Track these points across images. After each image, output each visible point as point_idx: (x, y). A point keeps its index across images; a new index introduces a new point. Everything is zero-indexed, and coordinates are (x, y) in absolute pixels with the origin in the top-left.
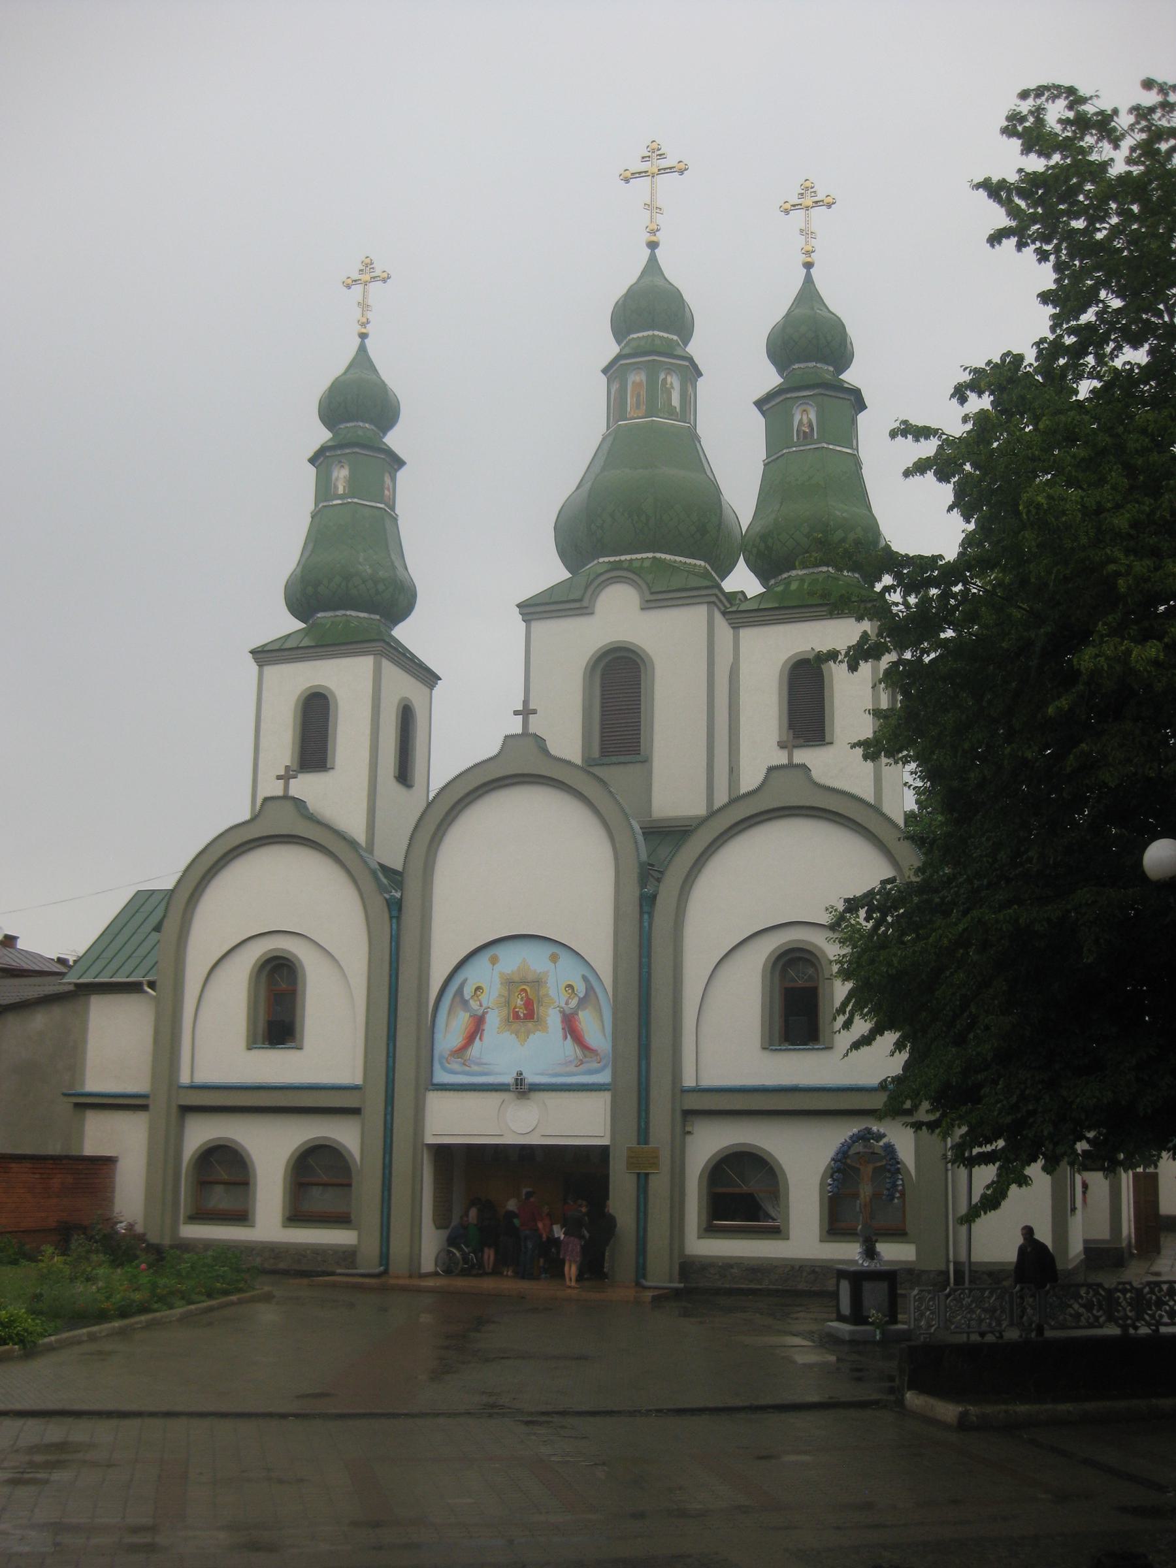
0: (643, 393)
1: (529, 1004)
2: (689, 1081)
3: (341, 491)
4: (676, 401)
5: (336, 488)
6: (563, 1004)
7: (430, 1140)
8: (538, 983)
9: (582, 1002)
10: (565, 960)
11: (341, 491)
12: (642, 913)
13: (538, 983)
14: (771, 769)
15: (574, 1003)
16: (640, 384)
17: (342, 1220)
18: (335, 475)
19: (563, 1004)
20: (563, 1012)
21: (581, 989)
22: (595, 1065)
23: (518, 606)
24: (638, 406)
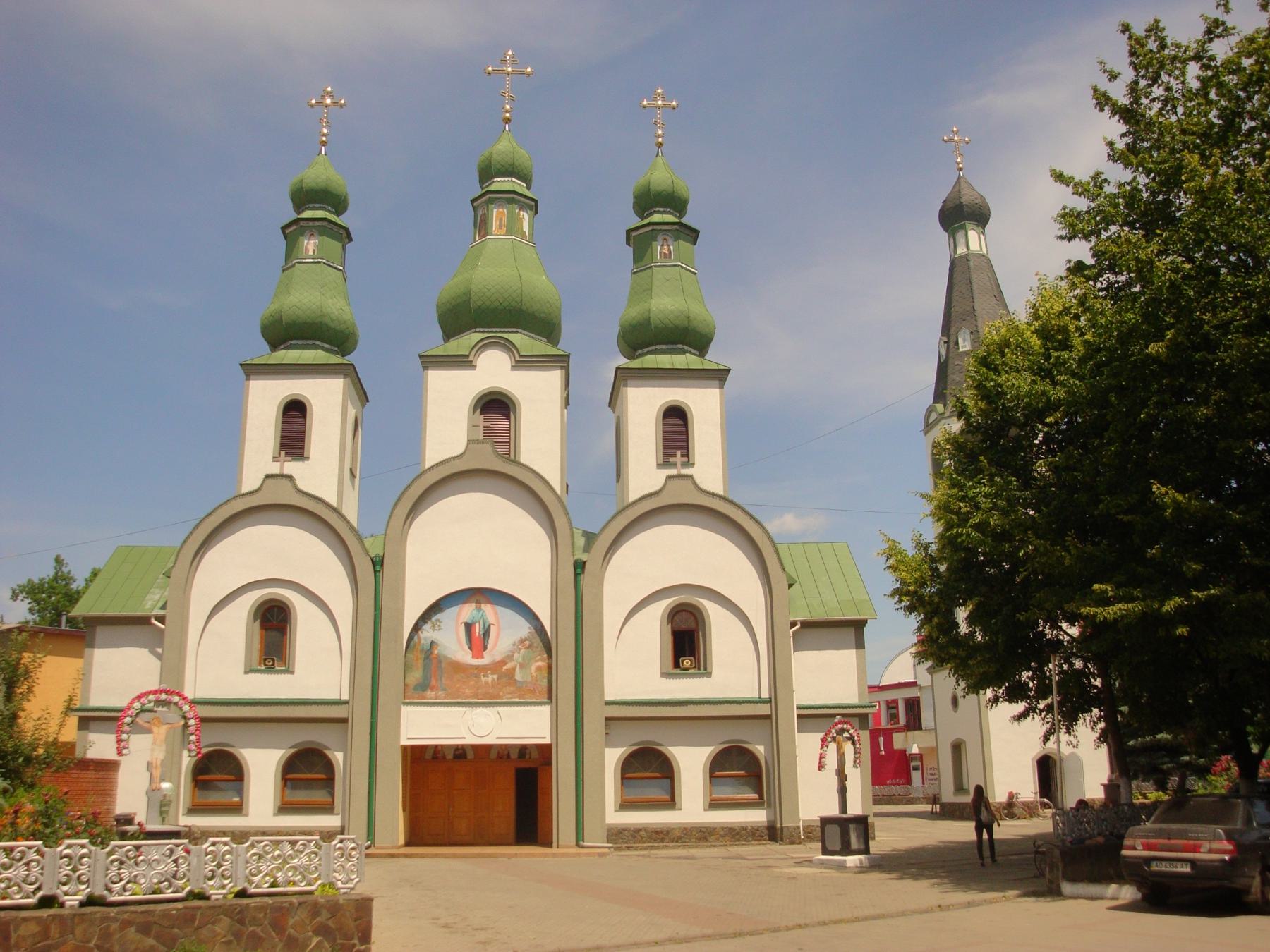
2: (608, 697)
3: (311, 253)
4: (526, 227)
5: (307, 250)
7: (404, 742)
14: (669, 477)
17: (328, 808)
23: (420, 356)
24: (500, 227)
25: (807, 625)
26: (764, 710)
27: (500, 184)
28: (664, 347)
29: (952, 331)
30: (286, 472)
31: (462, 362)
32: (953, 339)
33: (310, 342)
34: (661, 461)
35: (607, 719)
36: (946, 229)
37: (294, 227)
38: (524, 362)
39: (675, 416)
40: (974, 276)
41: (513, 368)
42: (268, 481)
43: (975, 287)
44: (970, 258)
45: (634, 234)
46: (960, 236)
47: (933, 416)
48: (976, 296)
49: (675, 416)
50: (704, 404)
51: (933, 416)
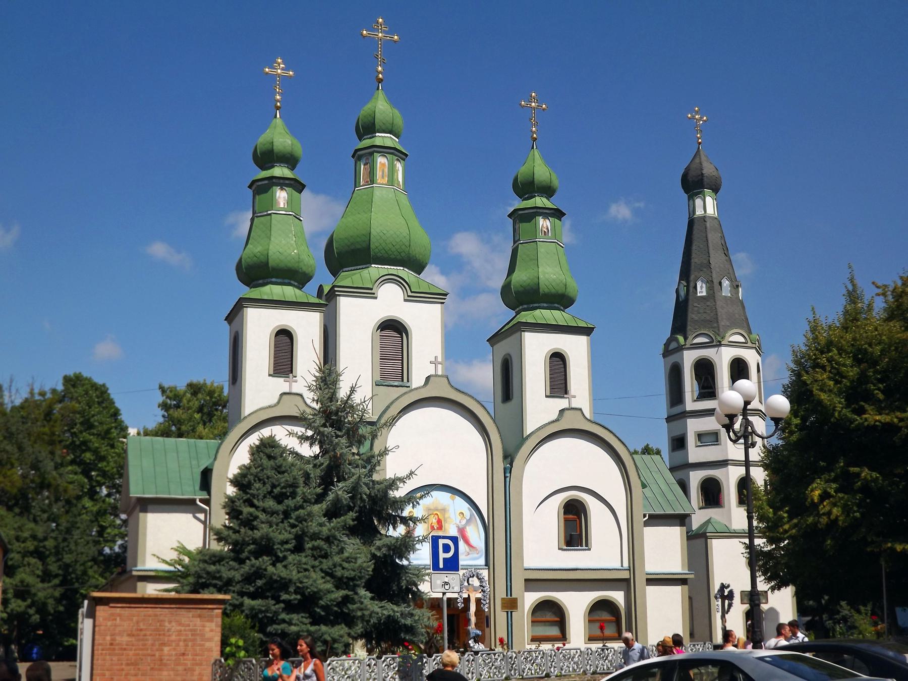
0: (386, 170)
1: (439, 522)
2: (527, 564)
6: (458, 522)
8: (444, 510)
9: (469, 522)
10: (459, 500)
11: (282, 206)
12: (505, 477)
13: (444, 510)
15: (464, 522)
16: (383, 165)
18: (278, 195)
19: (458, 522)
20: (458, 527)
21: (467, 514)
22: (476, 555)
24: (383, 177)
25: (651, 516)
26: (625, 575)
27: (382, 139)
28: (545, 305)
29: (692, 277)
30: (294, 391)
31: (367, 292)
32: (692, 285)
33: (286, 281)
34: (548, 394)
35: (526, 580)
36: (686, 192)
37: (266, 182)
38: (414, 296)
39: (558, 360)
40: (710, 236)
41: (405, 300)
42: (285, 397)
43: (710, 245)
44: (707, 219)
45: (520, 212)
46: (698, 202)
47: (673, 345)
48: (711, 251)
49: (558, 360)
50: (576, 348)
51: (673, 345)
